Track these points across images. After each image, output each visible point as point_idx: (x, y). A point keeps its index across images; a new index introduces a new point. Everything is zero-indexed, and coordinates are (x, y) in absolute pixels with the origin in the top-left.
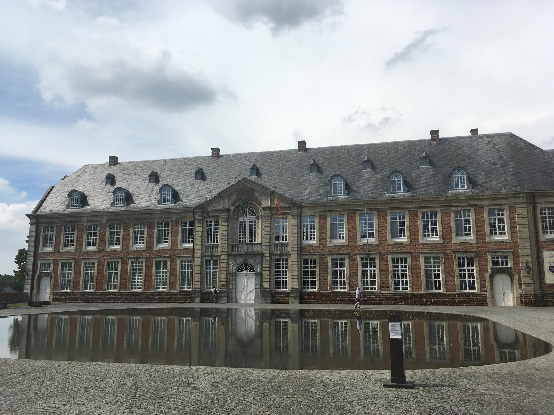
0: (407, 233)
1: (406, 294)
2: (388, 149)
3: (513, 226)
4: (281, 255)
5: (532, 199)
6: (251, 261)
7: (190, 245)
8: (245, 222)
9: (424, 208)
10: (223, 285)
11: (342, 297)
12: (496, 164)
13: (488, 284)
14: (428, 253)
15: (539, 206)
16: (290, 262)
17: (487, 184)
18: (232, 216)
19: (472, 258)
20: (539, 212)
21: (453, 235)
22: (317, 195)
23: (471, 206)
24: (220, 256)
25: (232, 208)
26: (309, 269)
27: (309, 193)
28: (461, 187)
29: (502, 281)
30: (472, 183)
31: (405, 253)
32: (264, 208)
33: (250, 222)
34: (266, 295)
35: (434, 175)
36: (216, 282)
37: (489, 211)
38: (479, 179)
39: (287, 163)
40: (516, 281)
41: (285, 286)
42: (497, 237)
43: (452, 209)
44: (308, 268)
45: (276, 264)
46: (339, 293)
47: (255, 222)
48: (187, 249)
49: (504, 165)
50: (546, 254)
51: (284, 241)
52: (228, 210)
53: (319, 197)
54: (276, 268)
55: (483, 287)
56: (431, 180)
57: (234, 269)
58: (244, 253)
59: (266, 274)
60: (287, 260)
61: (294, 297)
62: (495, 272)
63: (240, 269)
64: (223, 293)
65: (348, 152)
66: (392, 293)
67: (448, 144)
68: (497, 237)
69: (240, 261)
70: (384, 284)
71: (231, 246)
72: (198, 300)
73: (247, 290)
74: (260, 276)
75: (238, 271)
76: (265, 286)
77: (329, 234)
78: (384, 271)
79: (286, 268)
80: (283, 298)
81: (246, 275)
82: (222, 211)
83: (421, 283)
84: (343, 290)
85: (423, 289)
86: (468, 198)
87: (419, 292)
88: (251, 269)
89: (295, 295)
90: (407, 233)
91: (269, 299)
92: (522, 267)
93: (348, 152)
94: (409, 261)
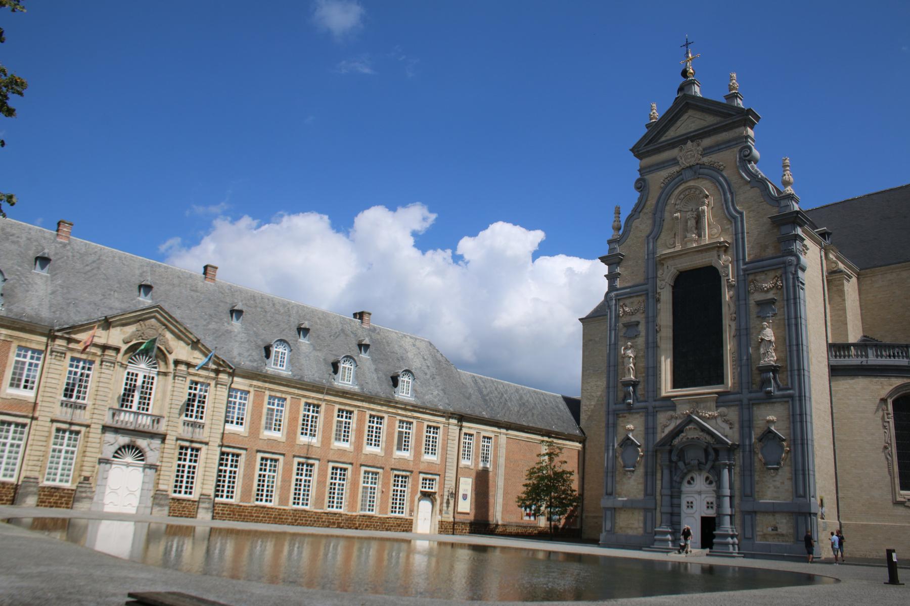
0: (382, 444)
1: (341, 515)
2: (319, 318)
6: (142, 443)
7: (29, 395)
8: (137, 375)
9: (373, 410)
10: (87, 479)
12: (426, 374)
13: (415, 508)
15: (464, 430)
16: (202, 455)
17: (424, 395)
19: (406, 477)
20: (462, 436)
21: (395, 448)
22: (250, 361)
23: (414, 418)
24: (88, 426)
25: (124, 348)
26: (228, 468)
27: (240, 354)
29: (426, 505)
31: (378, 468)
32: (177, 363)
33: (145, 377)
34: (162, 502)
35: (376, 370)
36: (50, 468)
37: (271, 397)
39: (195, 295)
40: (438, 507)
41: (189, 490)
43: (399, 418)
44: (226, 465)
45: (181, 454)
46: (264, 507)
47: (153, 378)
48: (19, 402)
50: (462, 480)
51: (199, 420)
52: (117, 350)
53: (255, 364)
54: (180, 459)
55: (411, 511)
56: (375, 376)
57: (109, 452)
58: (132, 428)
60: (198, 450)
61: (206, 508)
62: (426, 495)
63: (118, 452)
64: (85, 492)
65: (274, 305)
67: (378, 333)
69: (123, 440)
70: (319, 501)
71: (111, 412)
72: (31, 501)
73: (124, 489)
75: (114, 457)
76: (161, 487)
78: (321, 483)
79: (195, 461)
81: (128, 465)
82: (104, 348)
83: (356, 502)
84: (268, 504)
87: (354, 514)
88: (140, 454)
89: (206, 505)
90: (352, 437)
91: (167, 508)
93: (274, 305)
94: (349, 473)
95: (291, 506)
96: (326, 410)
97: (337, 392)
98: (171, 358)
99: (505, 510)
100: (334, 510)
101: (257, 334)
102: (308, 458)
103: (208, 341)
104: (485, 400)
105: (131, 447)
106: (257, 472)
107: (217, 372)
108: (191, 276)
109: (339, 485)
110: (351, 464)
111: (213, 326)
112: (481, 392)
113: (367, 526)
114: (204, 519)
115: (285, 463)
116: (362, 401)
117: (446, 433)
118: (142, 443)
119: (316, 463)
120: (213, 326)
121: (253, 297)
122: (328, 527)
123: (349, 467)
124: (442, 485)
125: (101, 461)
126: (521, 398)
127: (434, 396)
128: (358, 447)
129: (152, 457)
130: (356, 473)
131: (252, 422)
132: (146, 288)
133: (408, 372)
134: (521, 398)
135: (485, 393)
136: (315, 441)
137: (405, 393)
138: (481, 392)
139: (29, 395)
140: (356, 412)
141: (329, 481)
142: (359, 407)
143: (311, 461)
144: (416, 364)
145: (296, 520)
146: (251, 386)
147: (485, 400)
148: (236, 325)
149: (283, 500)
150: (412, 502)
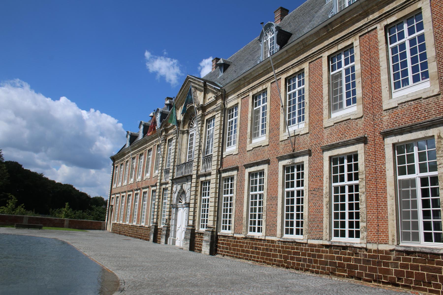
1: (354, 250)
11: (256, 248)
14: (401, 131)
46: (253, 239)
66: (327, 246)
78: (316, 191)
85: (390, 238)
87: (382, 247)
97: (317, 33)
100: (346, 240)
102: (293, 156)
109: (351, 187)
110: (363, 140)
113: (420, 280)
115: (270, 175)
116: (366, 15)
119: (305, 159)
122: (333, 273)
123: (359, 148)
128: (373, 101)
130: (376, 156)
136: (300, 127)
140: (356, 43)
142: (359, 30)
143: (298, 160)
145: (286, 258)
146: (238, 96)
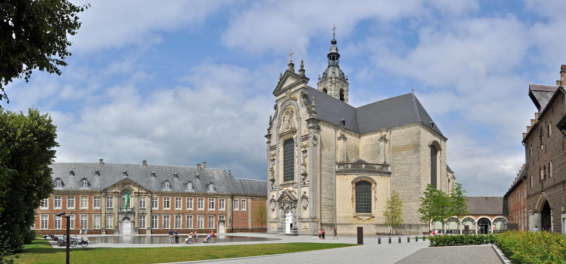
3: (226, 206)
4: (143, 214)
5: (232, 197)
18: (120, 195)
28: (211, 190)
30: (215, 189)
32: (135, 193)
38: (217, 188)
41: (144, 227)
42: (221, 209)
48: (97, 210)
49: (223, 183)
52: (118, 192)
55: (216, 227)
57: (121, 219)
59: (136, 221)
62: (220, 221)
63: (123, 219)
68: (221, 209)
70: (183, 226)
74: (134, 222)
77: (163, 205)
78: (184, 221)
80: (144, 232)
82: (115, 192)
86: (214, 195)
88: (129, 219)
92: (228, 220)
95: (175, 228)
96: (183, 200)
98: (133, 192)
99: (252, 223)
101: (160, 179)
103: (144, 185)
104: (243, 188)
105: (127, 218)
106: (175, 220)
107: (147, 193)
108: (139, 165)
111: (146, 180)
112: (242, 184)
114: (149, 234)
117: (226, 201)
118: (129, 216)
120: (146, 180)
121: (159, 168)
124: (226, 218)
125: (121, 222)
126: (260, 185)
127: (222, 189)
129: (132, 219)
131: (160, 206)
132: (125, 173)
133: (211, 183)
134: (260, 185)
135: (244, 184)
137: (211, 190)
138: (242, 184)
139: (99, 208)
141: (186, 220)
144: (217, 178)
147: (243, 188)
148: (153, 178)
149: (172, 226)
150: (216, 224)
